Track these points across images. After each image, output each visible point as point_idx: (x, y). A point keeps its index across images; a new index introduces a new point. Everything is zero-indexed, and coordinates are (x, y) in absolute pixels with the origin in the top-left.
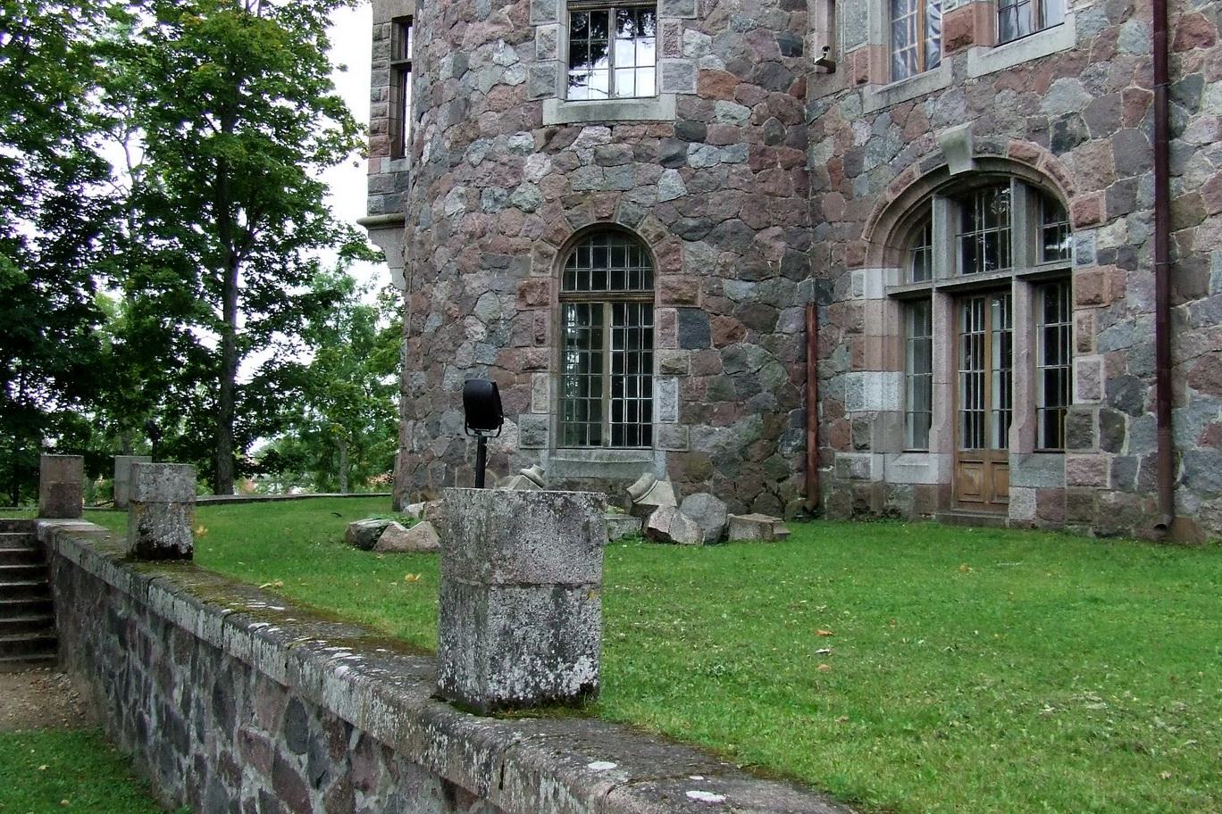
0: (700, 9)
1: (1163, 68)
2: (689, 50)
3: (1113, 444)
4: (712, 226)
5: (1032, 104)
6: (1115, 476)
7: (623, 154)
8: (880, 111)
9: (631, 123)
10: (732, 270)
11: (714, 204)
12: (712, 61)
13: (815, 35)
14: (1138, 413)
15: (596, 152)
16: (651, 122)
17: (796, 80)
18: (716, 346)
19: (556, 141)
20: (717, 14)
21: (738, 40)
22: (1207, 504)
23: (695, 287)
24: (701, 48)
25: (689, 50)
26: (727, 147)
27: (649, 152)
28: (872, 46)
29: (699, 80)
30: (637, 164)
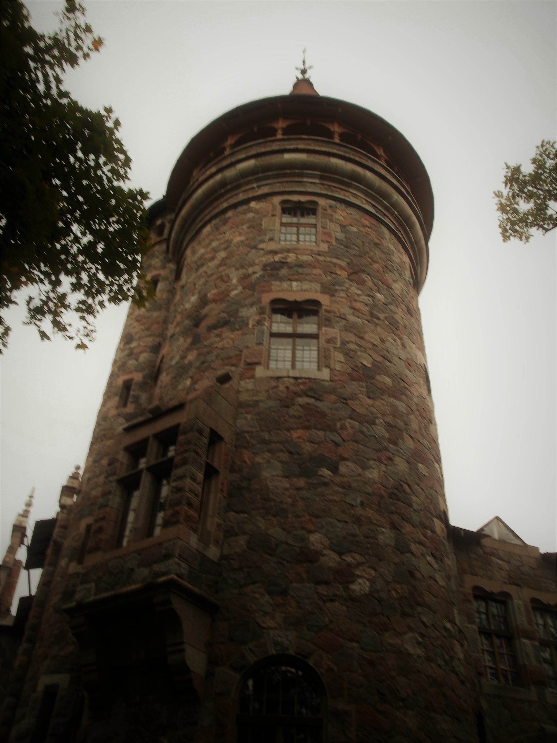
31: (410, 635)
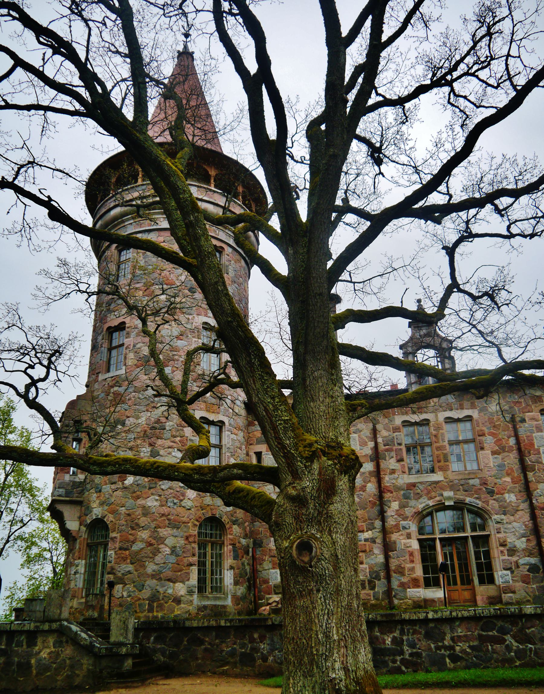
1: (381, 497)
3: (373, 588)
6: (374, 596)
14: (379, 580)
22: (401, 602)
31: (152, 497)
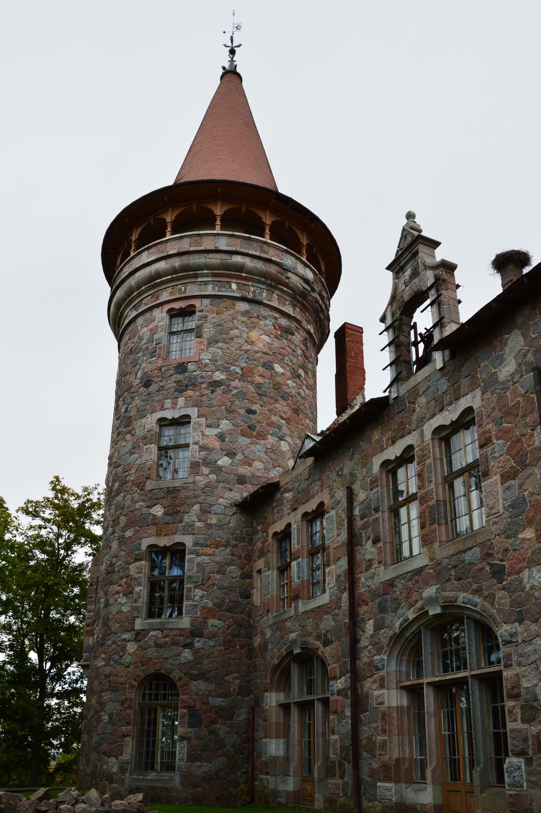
0: (202, 581)
2: (197, 598)
4: (205, 674)
5: (317, 625)
7: (166, 643)
8: (274, 624)
9: (171, 629)
10: (213, 693)
11: (206, 664)
12: (207, 602)
13: (255, 590)
15: (155, 642)
16: (179, 629)
17: (247, 609)
18: (205, 727)
19: (140, 636)
20: (210, 583)
21: (219, 593)
23: (195, 701)
24: (202, 597)
25: (197, 598)
26: (213, 640)
27: (177, 642)
28: (272, 596)
29: (201, 610)
30: (172, 647)
